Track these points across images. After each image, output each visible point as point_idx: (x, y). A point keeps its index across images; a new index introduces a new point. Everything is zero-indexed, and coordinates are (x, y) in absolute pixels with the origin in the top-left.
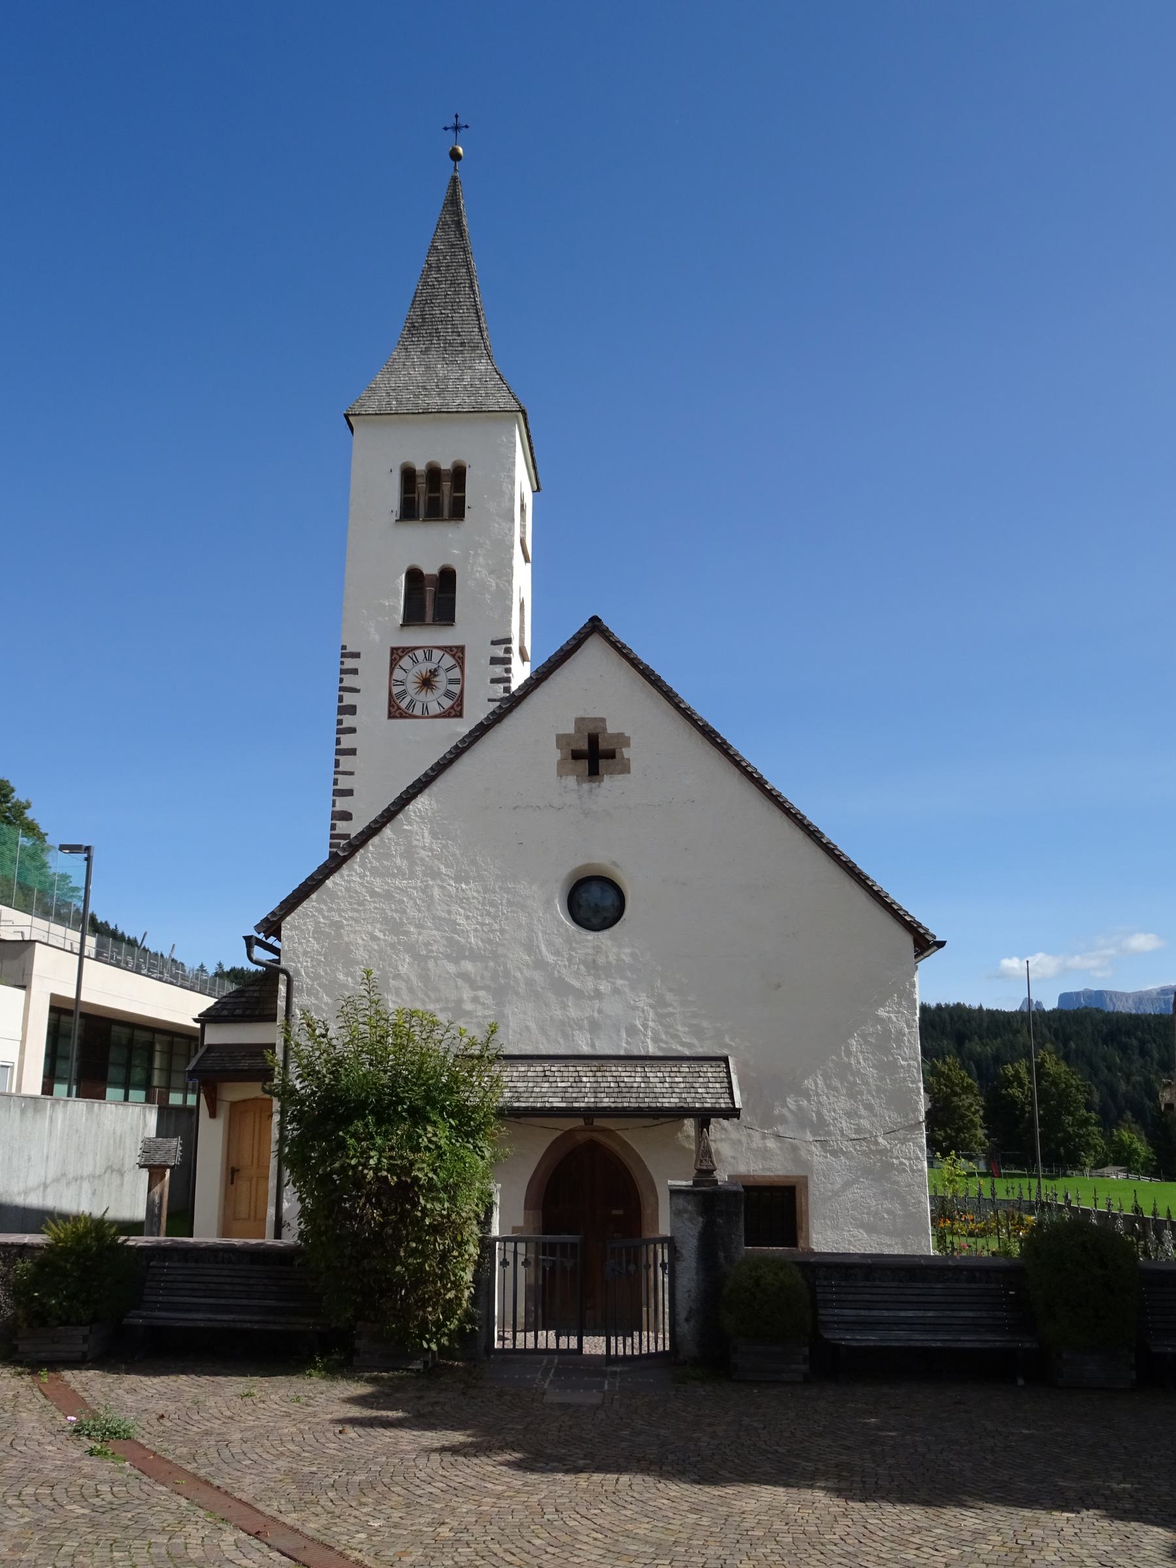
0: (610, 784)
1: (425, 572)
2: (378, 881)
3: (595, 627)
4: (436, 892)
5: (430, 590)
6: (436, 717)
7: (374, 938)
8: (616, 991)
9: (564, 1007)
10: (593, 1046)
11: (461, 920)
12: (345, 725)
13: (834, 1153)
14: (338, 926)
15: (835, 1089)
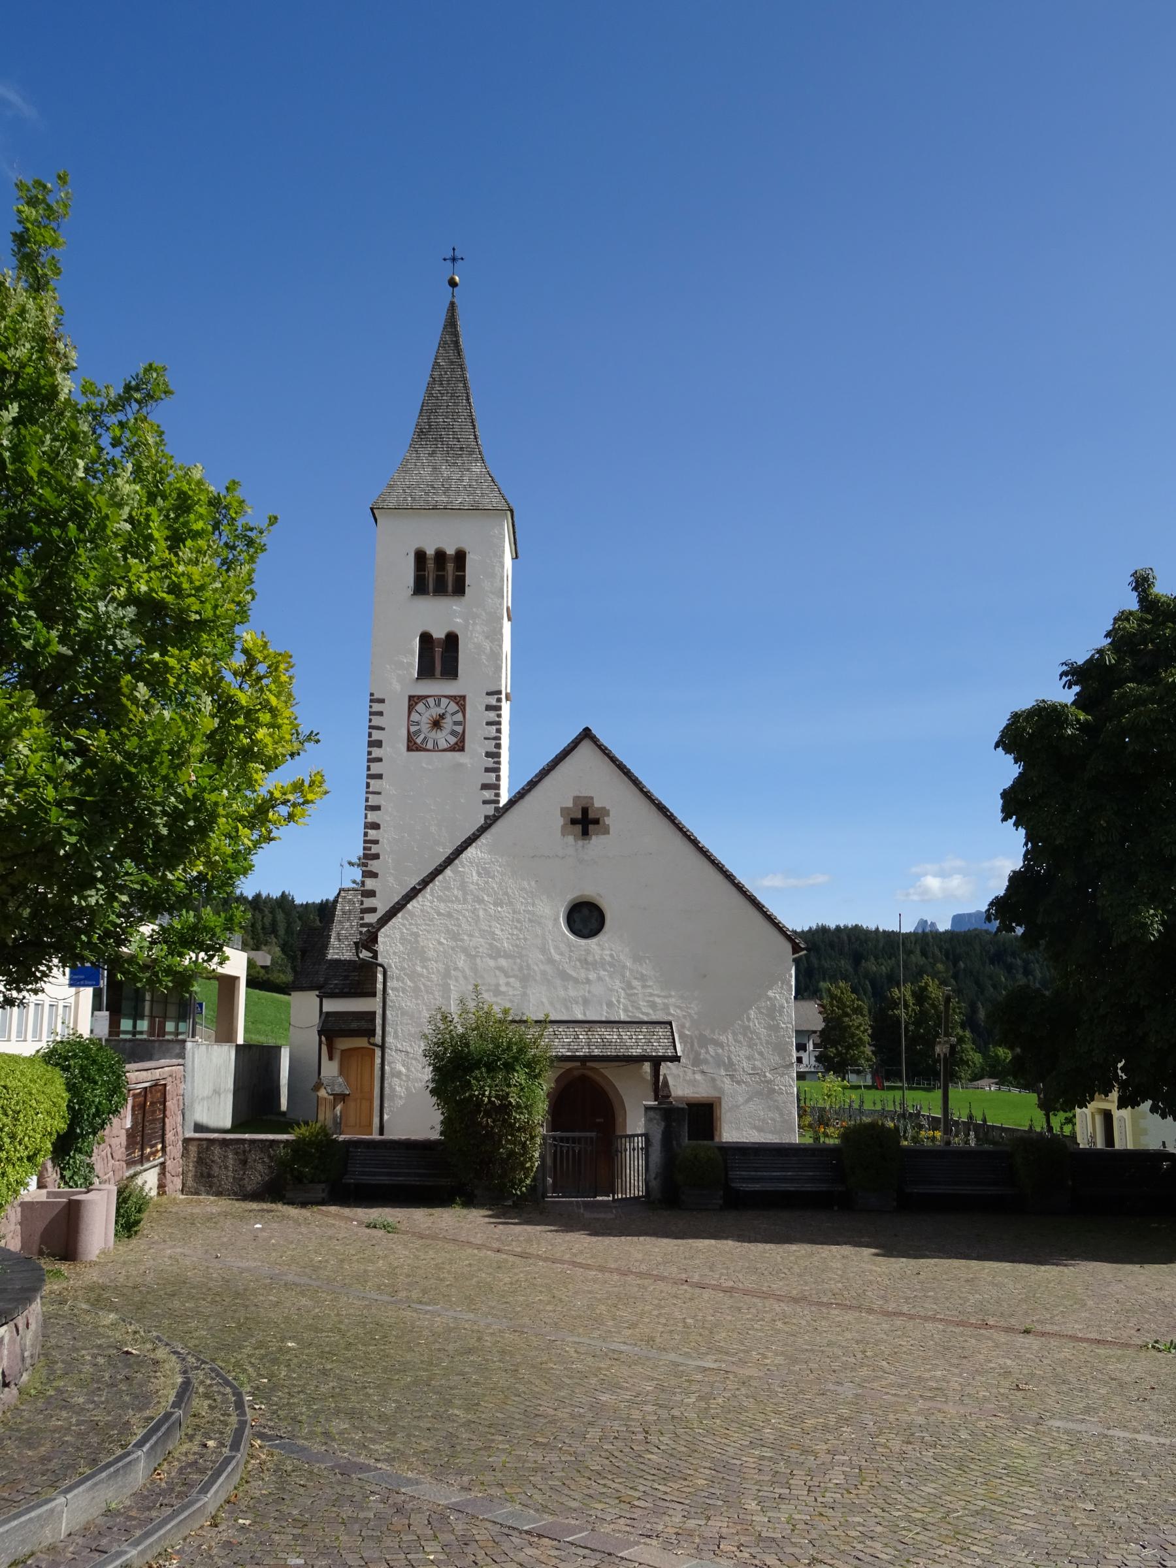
0: (597, 841)
1: (435, 636)
2: (442, 905)
3: (587, 734)
4: (481, 913)
5: (438, 650)
7: (440, 943)
8: (600, 979)
9: (566, 989)
10: (585, 1014)
11: (498, 932)
12: (374, 755)
13: (738, 1083)
14: (416, 935)
15: (740, 1042)
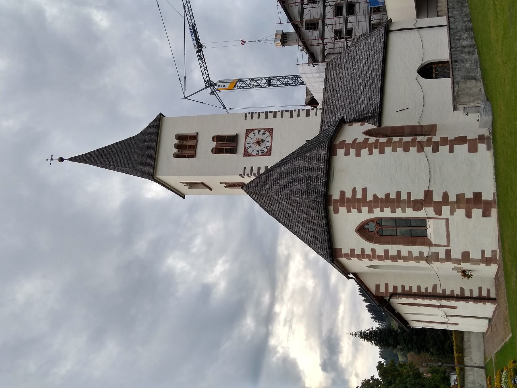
6: (272, 138)
